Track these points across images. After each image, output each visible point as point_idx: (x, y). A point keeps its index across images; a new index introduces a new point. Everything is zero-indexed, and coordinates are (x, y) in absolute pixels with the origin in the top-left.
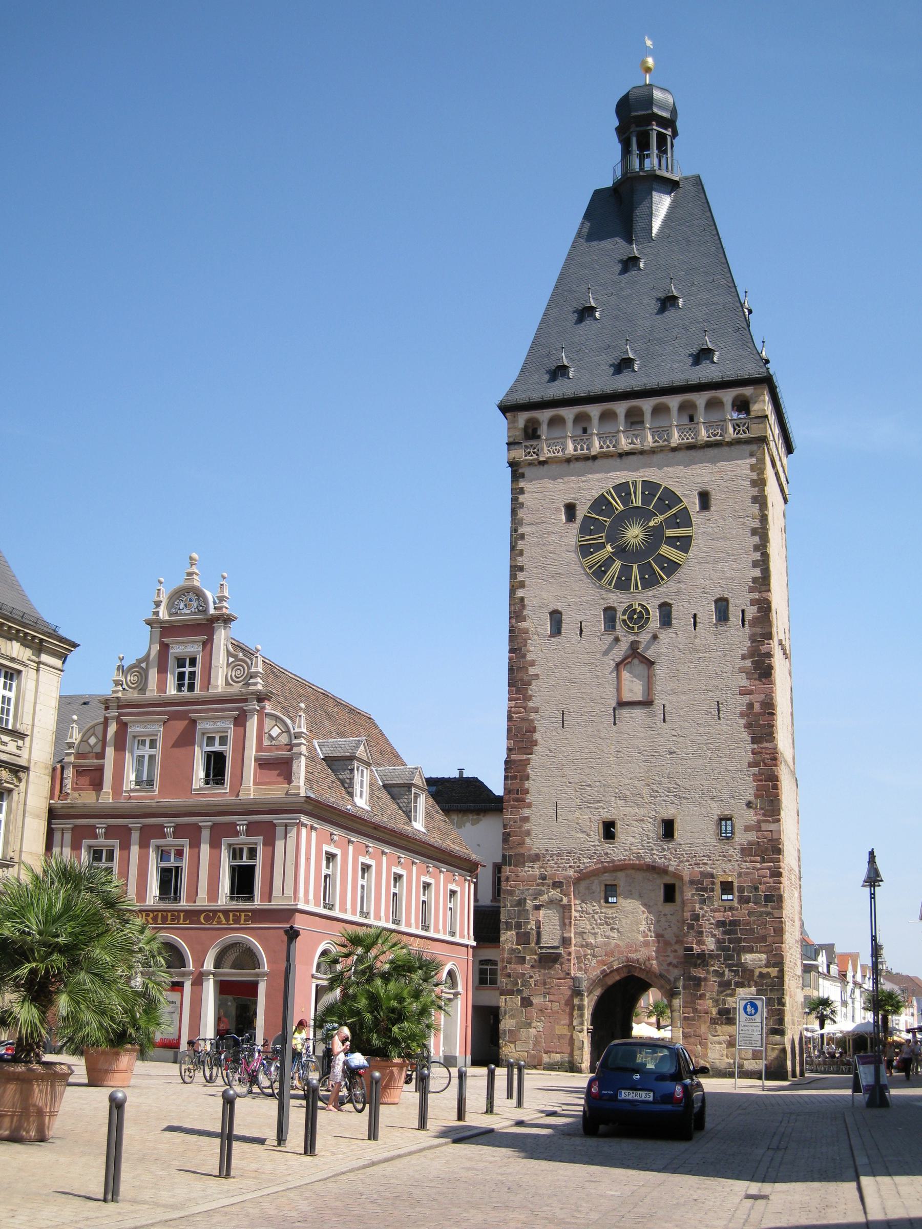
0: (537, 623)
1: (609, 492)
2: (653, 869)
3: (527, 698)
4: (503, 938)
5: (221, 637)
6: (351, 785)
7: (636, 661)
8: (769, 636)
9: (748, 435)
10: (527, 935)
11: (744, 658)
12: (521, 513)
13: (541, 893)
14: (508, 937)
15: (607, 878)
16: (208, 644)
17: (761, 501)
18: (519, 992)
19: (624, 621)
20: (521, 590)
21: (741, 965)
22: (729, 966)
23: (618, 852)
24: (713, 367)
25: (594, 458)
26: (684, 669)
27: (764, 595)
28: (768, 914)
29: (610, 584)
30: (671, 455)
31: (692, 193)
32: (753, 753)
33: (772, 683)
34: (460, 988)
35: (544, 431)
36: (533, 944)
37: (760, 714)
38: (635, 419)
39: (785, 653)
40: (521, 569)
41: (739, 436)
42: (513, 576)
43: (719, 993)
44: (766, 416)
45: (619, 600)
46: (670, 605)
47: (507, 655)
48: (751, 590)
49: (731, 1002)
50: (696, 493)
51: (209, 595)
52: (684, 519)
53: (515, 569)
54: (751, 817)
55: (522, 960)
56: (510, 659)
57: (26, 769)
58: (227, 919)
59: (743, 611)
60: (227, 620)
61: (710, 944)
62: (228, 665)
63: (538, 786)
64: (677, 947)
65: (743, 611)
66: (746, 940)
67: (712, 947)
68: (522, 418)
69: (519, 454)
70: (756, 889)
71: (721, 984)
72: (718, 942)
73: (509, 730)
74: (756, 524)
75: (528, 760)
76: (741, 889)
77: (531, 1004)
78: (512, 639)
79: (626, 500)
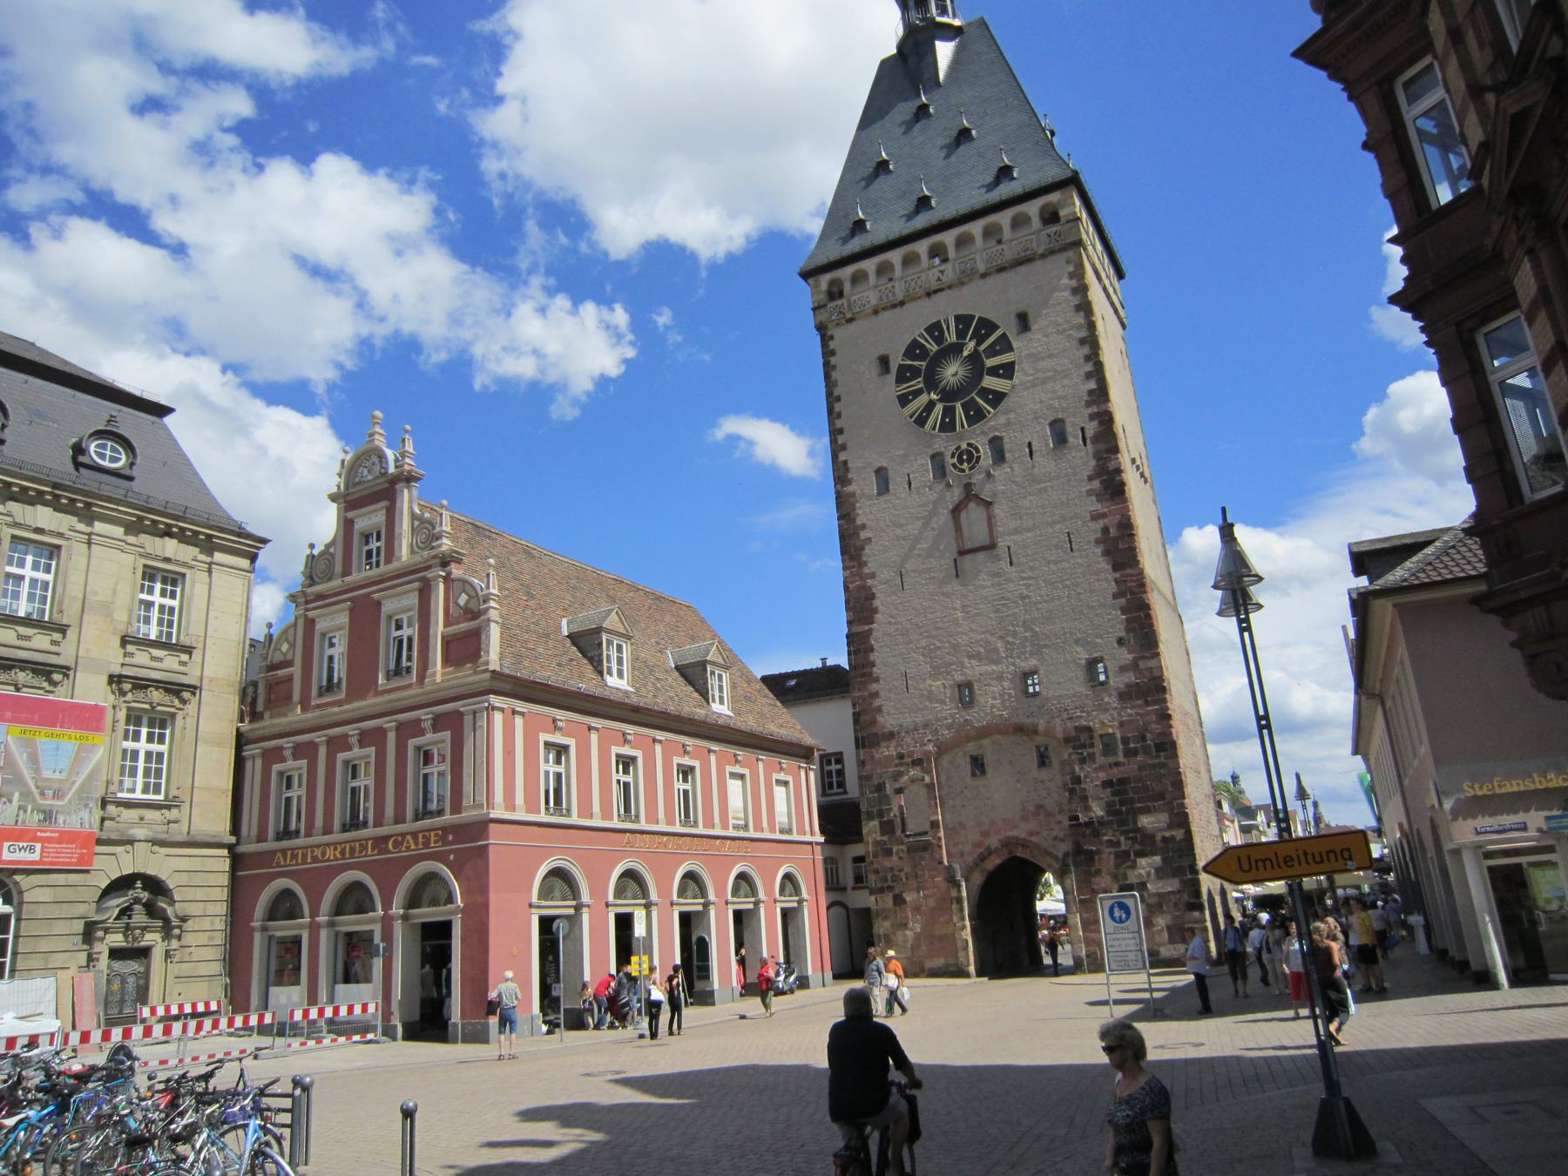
0: (862, 484)
1: (921, 335)
2: (1020, 729)
3: (862, 564)
4: (864, 832)
5: (408, 501)
7: (972, 505)
8: (1115, 450)
10: (891, 822)
11: (1090, 478)
12: (834, 375)
14: (871, 828)
15: (971, 748)
16: (391, 514)
17: (1085, 308)
18: (890, 888)
22: (1125, 833)
24: (1013, 183)
25: (902, 303)
26: (1026, 503)
27: (1103, 407)
28: (1163, 765)
30: (982, 282)
32: (1116, 581)
33: (1125, 501)
34: (805, 895)
35: (847, 287)
37: (1116, 539)
38: (937, 252)
39: (1142, 475)
40: (841, 431)
42: (833, 441)
43: (1118, 866)
44: (1079, 219)
45: (945, 444)
46: (1000, 439)
47: (836, 523)
48: (1088, 404)
49: (1132, 878)
50: (1013, 316)
51: (390, 454)
52: (1004, 345)
54: (1126, 656)
55: (889, 853)
57: (193, 689)
58: (416, 843)
59: (1083, 429)
60: (409, 479)
61: (1098, 811)
63: (883, 658)
65: (1083, 429)
67: (1100, 813)
68: (825, 279)
69: (823, 317)
70: (1144, 738)
71: (1117, 855)
73: (847, 602)
75: (871, 631)
76: (1125, 741)
77: (904, 902)
78: (839, 505)
79: (939, 340)
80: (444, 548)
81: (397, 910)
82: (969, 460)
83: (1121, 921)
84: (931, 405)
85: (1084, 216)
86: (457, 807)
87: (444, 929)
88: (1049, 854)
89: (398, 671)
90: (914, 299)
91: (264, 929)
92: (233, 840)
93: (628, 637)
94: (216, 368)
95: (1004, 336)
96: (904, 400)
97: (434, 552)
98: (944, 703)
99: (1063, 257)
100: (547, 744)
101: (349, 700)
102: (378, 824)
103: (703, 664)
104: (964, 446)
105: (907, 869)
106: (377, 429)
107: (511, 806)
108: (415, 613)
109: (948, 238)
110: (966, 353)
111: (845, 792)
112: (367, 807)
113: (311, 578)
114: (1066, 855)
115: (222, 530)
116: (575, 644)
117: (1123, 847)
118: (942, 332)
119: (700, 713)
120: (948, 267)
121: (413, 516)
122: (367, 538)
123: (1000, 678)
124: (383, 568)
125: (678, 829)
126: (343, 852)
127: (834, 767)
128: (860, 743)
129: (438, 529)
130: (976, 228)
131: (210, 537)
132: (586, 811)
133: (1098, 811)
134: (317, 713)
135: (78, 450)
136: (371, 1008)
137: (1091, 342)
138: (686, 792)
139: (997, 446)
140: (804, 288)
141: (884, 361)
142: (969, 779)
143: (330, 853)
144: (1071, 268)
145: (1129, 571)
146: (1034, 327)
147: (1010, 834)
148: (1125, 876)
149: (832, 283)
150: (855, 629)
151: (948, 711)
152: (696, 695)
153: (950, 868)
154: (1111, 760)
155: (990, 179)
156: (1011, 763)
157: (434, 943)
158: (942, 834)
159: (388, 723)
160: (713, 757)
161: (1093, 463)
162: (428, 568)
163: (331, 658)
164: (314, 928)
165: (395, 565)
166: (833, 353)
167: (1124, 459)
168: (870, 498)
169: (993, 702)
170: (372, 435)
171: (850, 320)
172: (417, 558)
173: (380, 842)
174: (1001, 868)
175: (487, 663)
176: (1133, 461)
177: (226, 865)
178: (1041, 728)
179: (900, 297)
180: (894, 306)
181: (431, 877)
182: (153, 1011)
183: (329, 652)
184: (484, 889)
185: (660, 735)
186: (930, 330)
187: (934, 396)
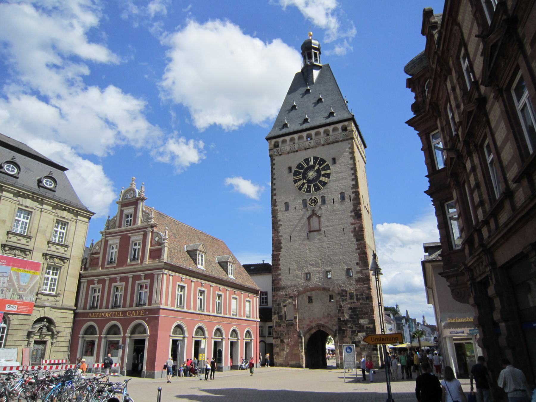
0: (281, 207)
2: (324, 289)
3: (278, 232)
4: (273, 318)
6: (196, 260)
7: (314, 217)
8: (359, 203)
11: (351, 212)
12: (274, 171)
13: (285, 301)
14: (275, 317)
15: (308, 294)
17: (353, 158)
18: (280, 337)
21: (359, 324)
22: (355, 325)
23: (311, 284)
24: (334, 118)
26: (331, 218)
28: (368, 304)
30: (322, 147)
31: (326, 70)
32: (357, 245)
33: (362, 220)
34: (253, 338)
35: (280, 144)
36: (284, 320)
37: (358, 231)
38: (309, 136)
39: (368, 211)
40: (275, 189)
42: (272, 192)
43: (352, 335)
44: (353, 131)
45: (307, 197)
46: (324, 196)
48: (352, 188)
49: (356, 339)
51: (137, 191)
52: (328, 167)
53: (273, 190)
54: (358, 269)
55: (280, 326)
57: (68, 259)
58: (136, 314)
60: (143, 199)
61: (347, 317)
62: (142, 215)
63: (283, 263)
64: (335, 318)
66: (360, 314)
67: (348, 318)
68: (273, 141)
69: (272, 152)
70: (362, 295)
71: (352, 332)
72: (350, 315)
73: (273, 244)
76: (357, 295)
77: (284, 342)
79: (308, 164)
80: (152, 222)
81: (128, 335)
82: (314, 203)
83: (349, 353)
84: (304, 184)
85: (355, 129)
86: (150, 304)
87: (143, 342)
88: (330, 329)
89: (134, 259)
90: (300, 150)
91: (83, 337)
92: (75, 308)
93: (205, 253)
94: (70, 148)
95: (328, 165)
96: (295, 182)
97: (149, 223)
98: (301, 279)
99: (347, 142)
100: (179, 285)
101: (118, 266)
102: (124, 307)
103: (227, 262)
104: (313, 198)
105: (286, 331)
106: (134, 182)
107: (167, 304)
108: (141, 241)
109: (313, 132)
110: (316, 169)
111: (267, 305)
112: (120, 302)
113: (108, 227)
114: (336, 330)
115: (81, 209)
116: (188, 254)
117: (354, 329)
118: (309, 161)
119: (225, 278)
120: (312, 141)
121: (143, 211)
122: (127, 216)
123: (319, 272)
124: (132, 226)
125: (215, 314)
126: (111, 315)
127: (264, 296)
128: (273, 290)
129: (150, 216)
130: (322, 130)
131: (77, 211)
132: (188, 307)
133: (347, 317)
134: (107, 270)
135: (40, 181)
136: (118, 365)
137: (354, 169)
138: (219, 303)
139: (323, 198)
140: (267, 143)
141: (290, 169)
142: (307, 304)
143: (107, 315)
144: (350, 146)
145: (361, 242)
146: (337, 163)
147: (319, 322)
148: (354, 339)
149: (276, 142)
150: (275, 253)
151: (302, 281)
152: (224, 272)
153: (299, 332)
154: (352, 301)
155: (327, 115)
156: (321, 300)
157: (138, 346)
158: (297, 321)
159: (130, 275)
160: (228, 292)
161: (353, 207)
162: (147, 228)
163: (112, 253)
164: (100, 339)
165: (136, 226)
166: (274, 164)
167: (362, 207)
168: (283, 211)
169: (316, 280)
170: (132, 184)
171: (280, 155)
172: (143, 225)
173: (124, 313)
174: (315, 333)
175: (163, 259)
176: (365, 207)
177: (72, 316)
178: (331, 289)
179: (296, 149)
180: (294, 152)
181: (139, 325)
182: (46, 361)
183: (112, 251)
184: (157, 330)
185: (213, 284)
186: (305, 160)
187: (305, 181)
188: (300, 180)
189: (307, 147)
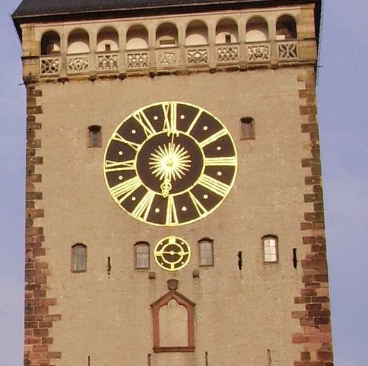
0: (56, 257)
8: (325, 277)
9: (295, 58)
11: (297, 301)
12: (38, 134)
19: (159, 258)
20: (40, 219)
25: (122, 77)
29: (142, 216)
40: (39, 196)
41: (286, 58)
42: (30, 204)
47: (23, 292)
48: (304, 227)
53: (32, 196)
56: (27, 297)
59: (295, 250)
65: (295, 250)
68: (40, 30)
69: (35, 68)
74: (308, 154)
78: (28, 275)
95: (225, 142)
96: (113, 179)
104: (172, 241)
161: (302, 286)
166: (39, 110)
179: (122, 70)
180: (115, 77)
186: (150, 112)
188: (129, 175)
189: (160, 67)
